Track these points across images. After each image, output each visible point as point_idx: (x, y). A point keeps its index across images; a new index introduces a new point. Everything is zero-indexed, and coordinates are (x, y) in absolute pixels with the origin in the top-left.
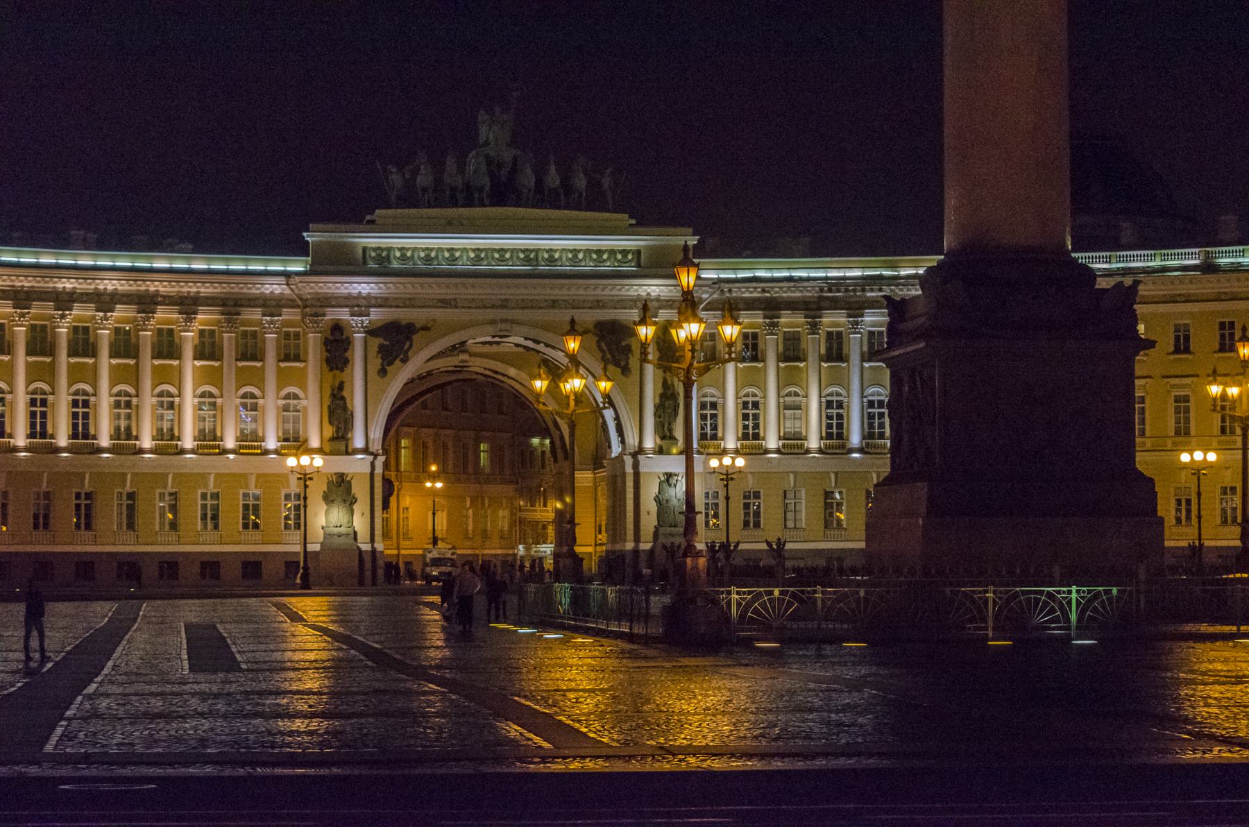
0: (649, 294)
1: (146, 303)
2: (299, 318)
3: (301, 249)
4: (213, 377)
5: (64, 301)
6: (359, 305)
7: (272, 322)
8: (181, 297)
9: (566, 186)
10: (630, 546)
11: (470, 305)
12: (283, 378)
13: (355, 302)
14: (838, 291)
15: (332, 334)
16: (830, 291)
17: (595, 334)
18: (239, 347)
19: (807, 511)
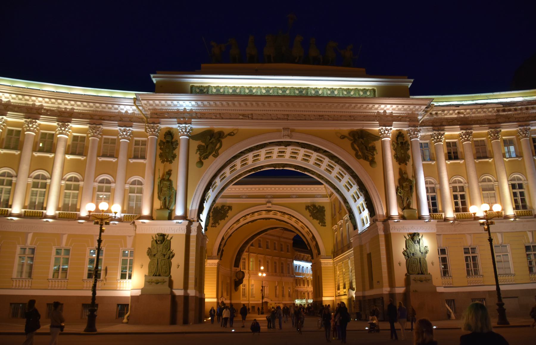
0: (385, 112)
1: (32, 112)
2: (144, 130)
4: (78, 167)
6: (183, 116)
7: (125, 131)
8: (59, 112)
10: (386, 290)
12: (130, 170)
13: (182, 115)
14: (510, 110)
15: (165, 138)
16: (504, 111)
17: (349, 139)
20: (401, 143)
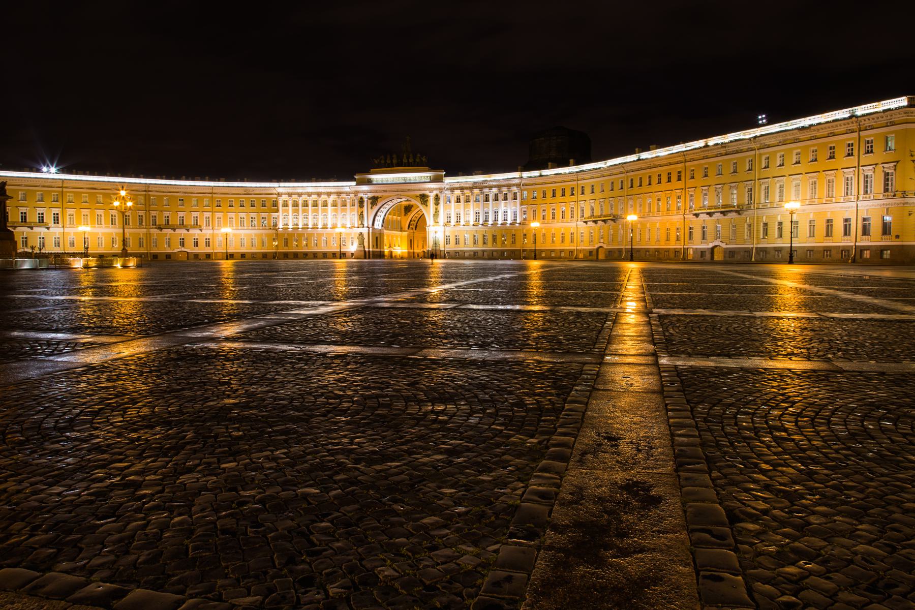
1: (319, 194)
3: (354, 180)
4: (336, 211)
5: (300, 195)
6: (365, 192)
9: (415, 161)
11: (391, 191)
12: (352, 211)
18: (341, 204)
19: (470, 241)
20: (437, 198)
